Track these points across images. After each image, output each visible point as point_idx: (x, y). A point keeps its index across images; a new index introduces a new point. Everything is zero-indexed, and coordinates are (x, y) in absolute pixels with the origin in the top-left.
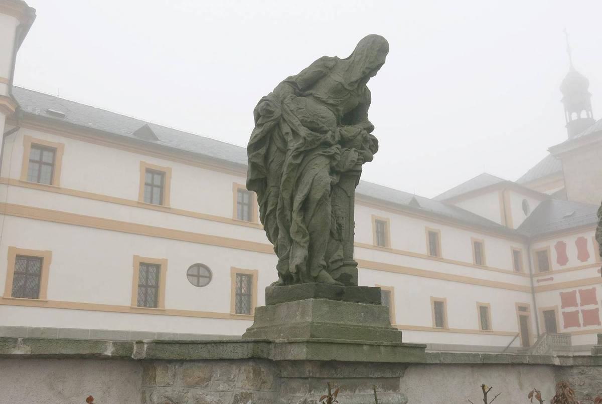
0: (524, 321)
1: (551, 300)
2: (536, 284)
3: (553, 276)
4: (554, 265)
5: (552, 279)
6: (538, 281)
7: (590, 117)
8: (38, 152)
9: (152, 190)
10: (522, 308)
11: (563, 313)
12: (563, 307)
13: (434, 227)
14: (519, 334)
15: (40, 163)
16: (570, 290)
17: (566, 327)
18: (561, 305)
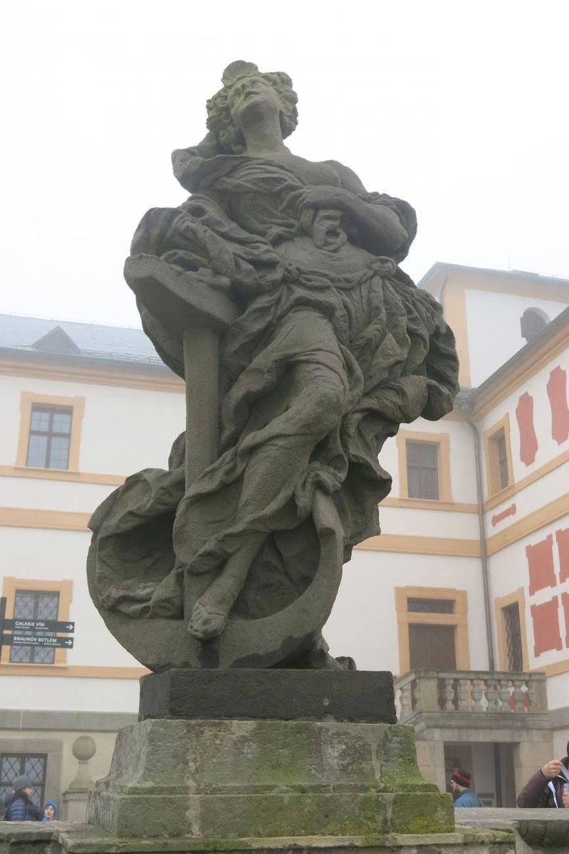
4: (519, 470)
5: (512, 510)
6: (496, 520)
8: (46, 416)
9: (49, 443)
11: (533, 608)
12: (532, 593)
15: (50, 434)
18: (528, 584)
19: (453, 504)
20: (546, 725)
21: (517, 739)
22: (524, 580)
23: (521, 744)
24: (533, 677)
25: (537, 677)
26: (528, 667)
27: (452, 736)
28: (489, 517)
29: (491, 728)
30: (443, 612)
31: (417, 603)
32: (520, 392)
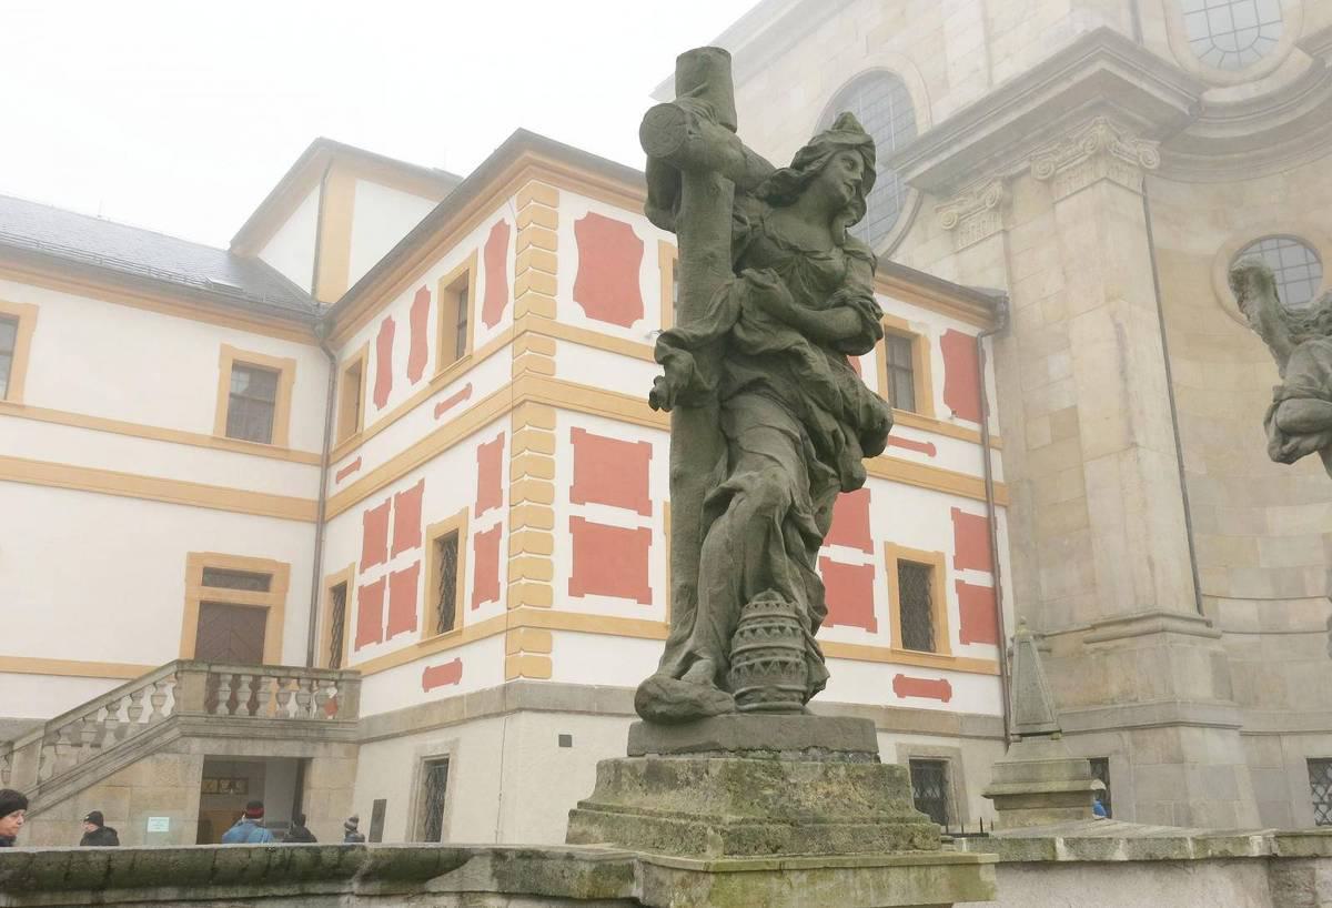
4: (371, 415)
6: (341, 475)
19: (288, 451)
20: (352, 736)
21: (308, 754)
23: (314, 760)
24: (344, 677)
25: (351, 677)
26: (347, 663)
27: (216, 748)
28: (335, 470)
29: (274, 739)
30: (253, 588)
31: (215, 575)
32: (383, 316)
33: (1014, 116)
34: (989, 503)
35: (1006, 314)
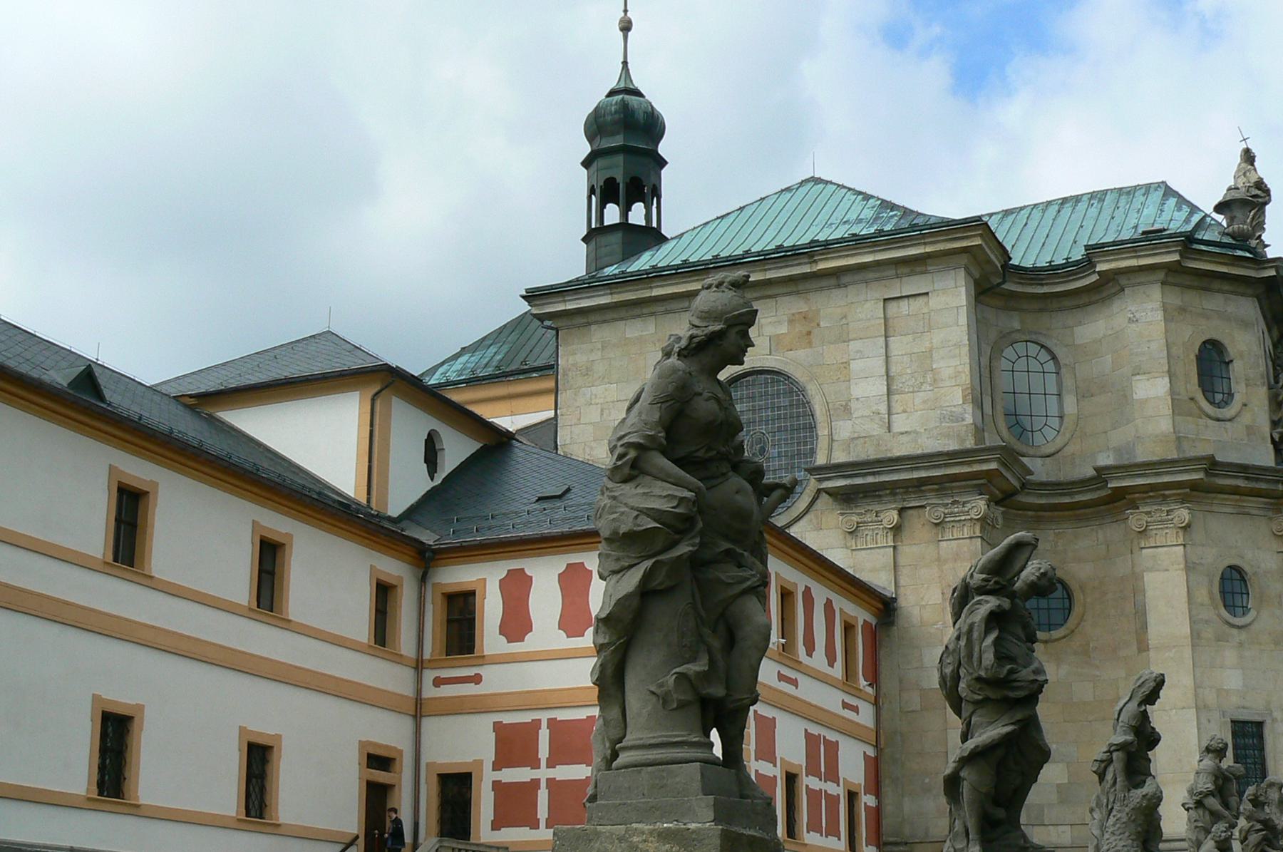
0: (377, 798)
1: (465, 743)
2: (430, 692)
3: (486, 671)
5: (477, 679)
6: (438, 682)
7: (654, 225)
10: (379, 760)
11: (497, 785)
12: (497, 766)
13: (139, 470)
14: (357, 837)
16: (526, 718)
17: (496, 826)
22: (489, 755)
28: (429, 675)
32: (515, 564)
33: (923, 474)
34: (876, 746)
35: (895, 610)
